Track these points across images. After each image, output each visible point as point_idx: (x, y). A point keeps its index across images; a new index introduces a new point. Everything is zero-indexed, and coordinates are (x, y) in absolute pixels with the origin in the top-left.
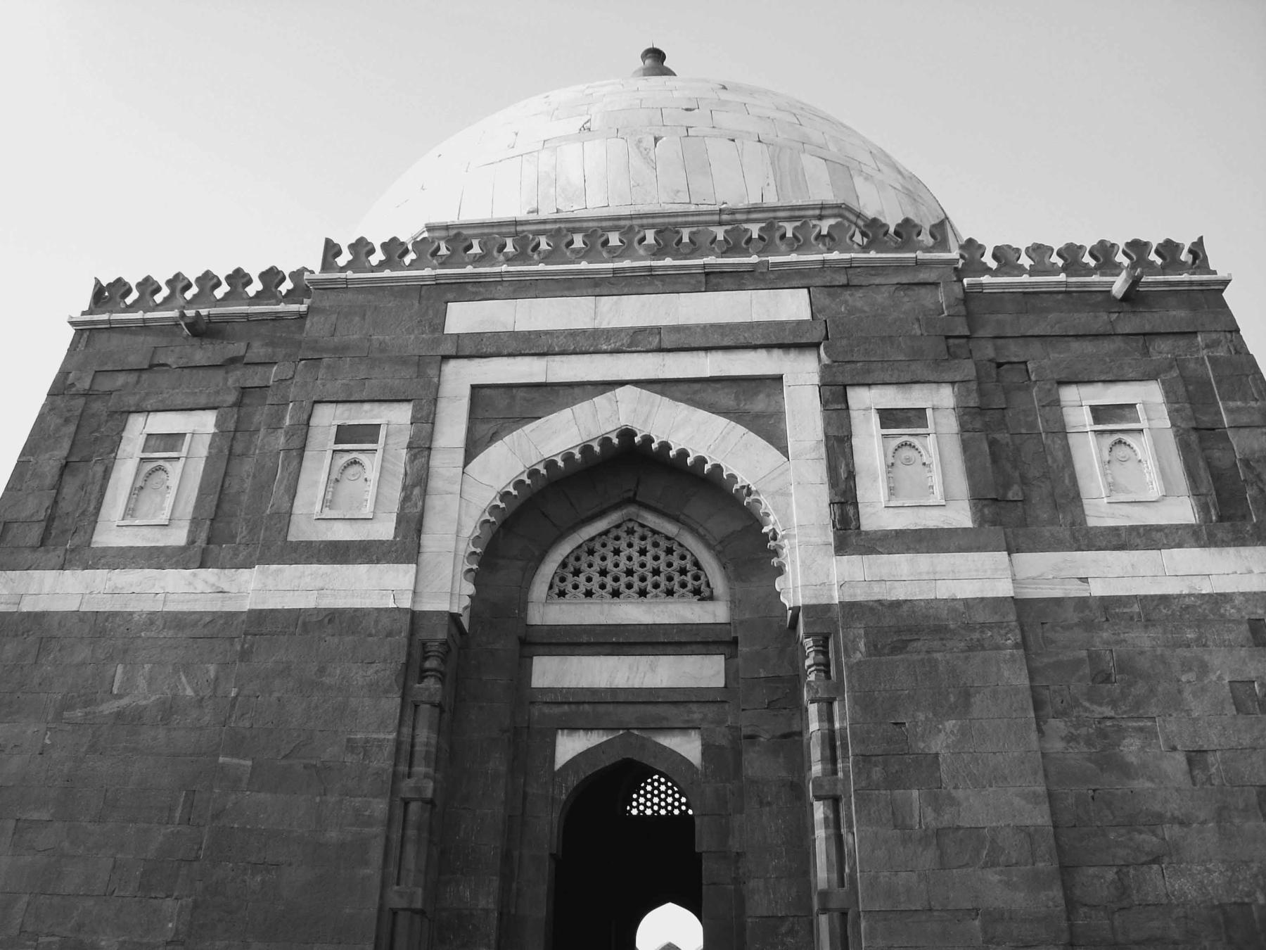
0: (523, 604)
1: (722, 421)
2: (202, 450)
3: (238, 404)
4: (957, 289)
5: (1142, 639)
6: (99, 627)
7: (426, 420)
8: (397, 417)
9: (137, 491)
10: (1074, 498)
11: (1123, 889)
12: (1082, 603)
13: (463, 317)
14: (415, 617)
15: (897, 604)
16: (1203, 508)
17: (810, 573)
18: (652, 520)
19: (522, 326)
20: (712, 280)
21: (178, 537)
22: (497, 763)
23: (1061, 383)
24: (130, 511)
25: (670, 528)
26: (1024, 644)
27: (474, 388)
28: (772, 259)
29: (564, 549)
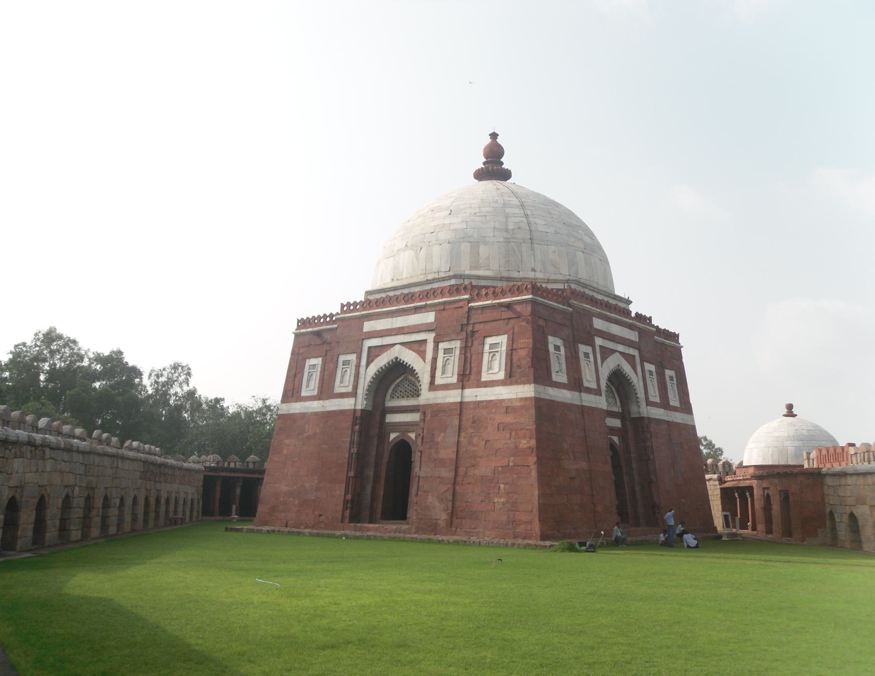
0: (384, 401)
1: (414, 354)
2: (319, 369)
3: (326, 355)
4: (466, 309)
5: (484, 412)
6: (303, 415)
7: (359, 358)
8: (353, 357)
9: (308, 380)
10: (479, 373)
11: (466, 473)
12: (475, 402)
13: (368, 326)
14: (355, 410)
15: (437, 404)
16: (506, 374)
17: (426, 397)
18: (410, 377)
19: (378, 328)
20: (417, 310)
21: (315, 393)
22: (375, 442)
23: (485, 337)
24: (307, 386)
25: (413, 379)
26: (460, 415)
27: (369, 348)
28: (429, 302)
29: (393, 386)
